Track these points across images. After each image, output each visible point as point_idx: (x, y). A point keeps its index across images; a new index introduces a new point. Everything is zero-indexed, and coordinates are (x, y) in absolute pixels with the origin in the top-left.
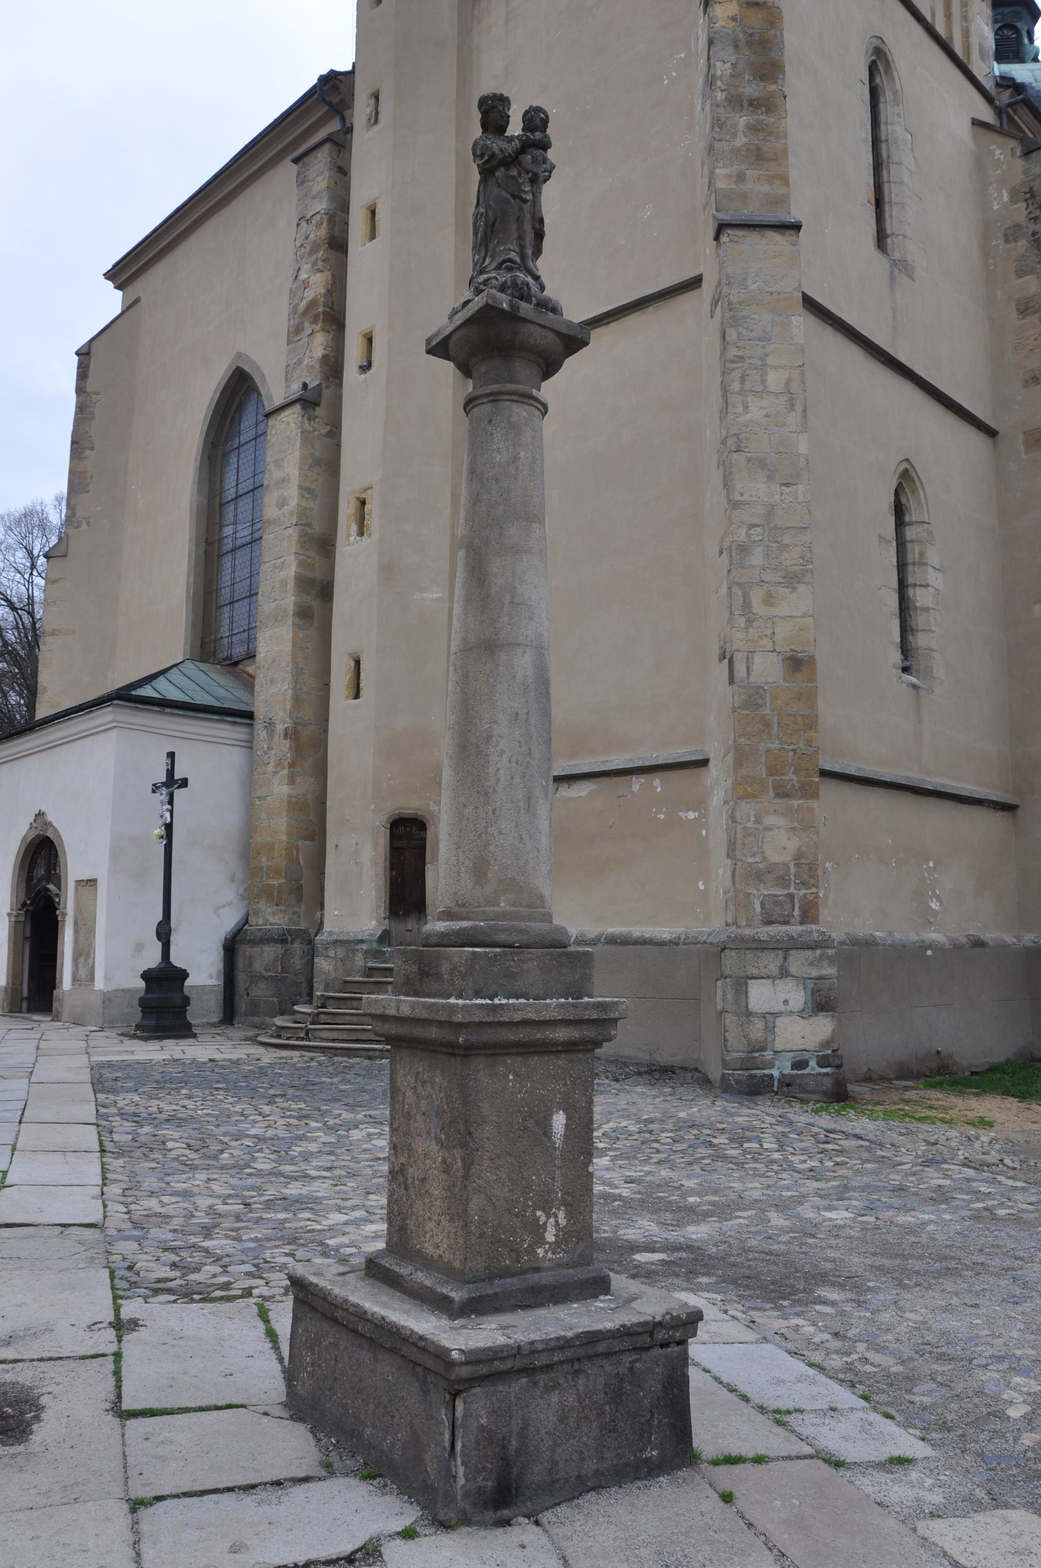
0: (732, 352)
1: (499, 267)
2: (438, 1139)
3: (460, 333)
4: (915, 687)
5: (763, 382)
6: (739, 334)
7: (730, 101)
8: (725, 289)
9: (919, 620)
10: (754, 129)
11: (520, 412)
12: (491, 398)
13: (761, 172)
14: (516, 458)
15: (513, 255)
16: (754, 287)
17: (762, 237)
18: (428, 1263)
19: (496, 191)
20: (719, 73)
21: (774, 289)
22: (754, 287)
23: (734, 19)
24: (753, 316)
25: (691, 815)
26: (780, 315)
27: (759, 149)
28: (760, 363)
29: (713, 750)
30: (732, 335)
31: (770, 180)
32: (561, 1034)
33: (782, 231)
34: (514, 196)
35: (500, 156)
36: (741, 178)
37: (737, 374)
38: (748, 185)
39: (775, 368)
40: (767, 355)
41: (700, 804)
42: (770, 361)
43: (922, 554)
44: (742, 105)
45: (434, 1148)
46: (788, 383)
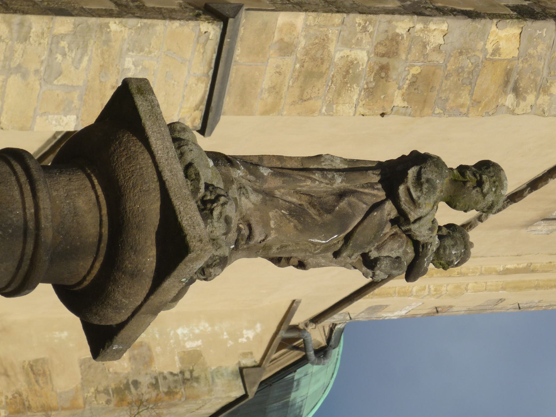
6: (62, 37)
7: (392, 40)
10: (349, 72)
12: (31, 225)
13: (288, 76)
17: (199, 79)
20: (432, 26)
23: (496, 51)
24: (86, 59)
27: (321, 75)
28: (13, 65)
31: (275, 89)
33: (203, 107)
34: (347, 238)
35: (413, 216)
36: (286, 49)
38: (274, 60)
40: (24, 76)
44: (383, 56)
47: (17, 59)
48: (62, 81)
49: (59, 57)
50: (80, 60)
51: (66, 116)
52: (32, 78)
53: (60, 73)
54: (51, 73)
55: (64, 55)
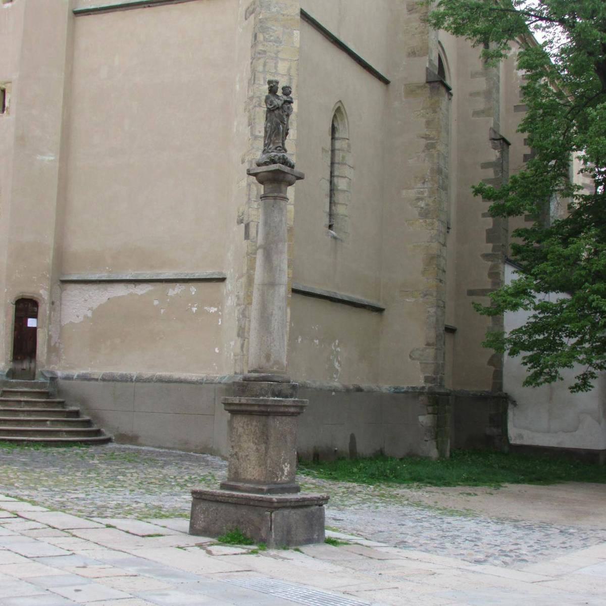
0: (260, 48)
1: (276, 149)
2: (254, 442)
3: (265, 173)
4: (335, 238)
5: (276, 67)
6: (264, 37)
8: (258, 9)
9: (339, 197)
11: (283, 203)
14: (281, 221)
15: (281, 145)
16: (274, 10)
18: (249, 481)
19: (275, 119)
21: (285, 13)
22: (274, 10)
24: (273, 27)
25: (213, 310)
26: (288, 29)
28: (275, 56)
29: (228, 273)
30: (261, 37)
32: (292, 410)
37: (262, 61)
39: (283, 60)
40: (279, 52)
41: (219, 303)
42: (280, 55)
43: (343, 157)
45: (252, 445)
46: (289, 69)
47: (273, 55)
48: (281, 36)
49: (272, 38)
50: (273, 29)
51: (294, 34)
52: (280, 49)
53: (278, 37)
54: (278, 41)
55: (271, 36)
